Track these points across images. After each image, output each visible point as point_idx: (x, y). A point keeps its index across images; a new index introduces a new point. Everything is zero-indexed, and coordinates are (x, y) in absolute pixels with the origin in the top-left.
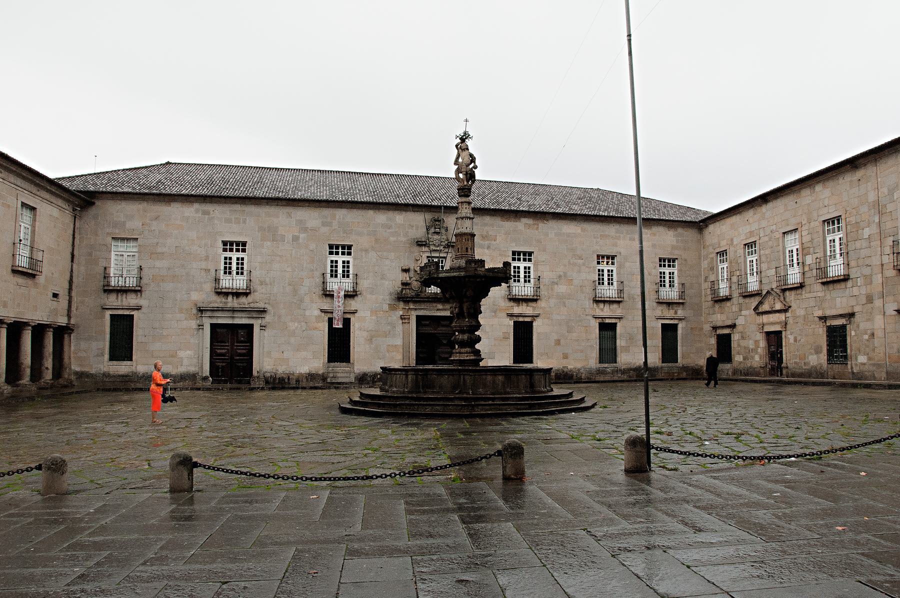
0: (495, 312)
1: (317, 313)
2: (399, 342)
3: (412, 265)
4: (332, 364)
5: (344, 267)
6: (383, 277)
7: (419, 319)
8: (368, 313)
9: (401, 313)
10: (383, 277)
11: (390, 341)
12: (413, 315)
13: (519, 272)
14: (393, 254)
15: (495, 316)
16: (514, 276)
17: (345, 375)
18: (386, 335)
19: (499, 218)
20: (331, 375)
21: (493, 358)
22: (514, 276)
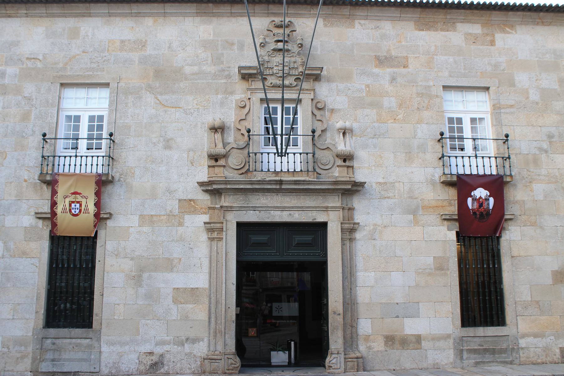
0: (414, 212)
1: (28, 220)
2: (200, 280)
3: (230, 117)
4: (52, 331)
5: (91, 128)
6: (168, 145)
7: (243, 228)
8: (135, 220)
9: (206, 218)
10: (168, 145)
11: (180, 280)
12: (232, 220)
13: (461, 130)
14: (190, 98)
15: (416, 222)
16: (452, 138)
17: (80, 355)
18: (169, 265)
19: (411, 25)
20: (49, 356)
21: (415, 315)
22: (452, 138)
